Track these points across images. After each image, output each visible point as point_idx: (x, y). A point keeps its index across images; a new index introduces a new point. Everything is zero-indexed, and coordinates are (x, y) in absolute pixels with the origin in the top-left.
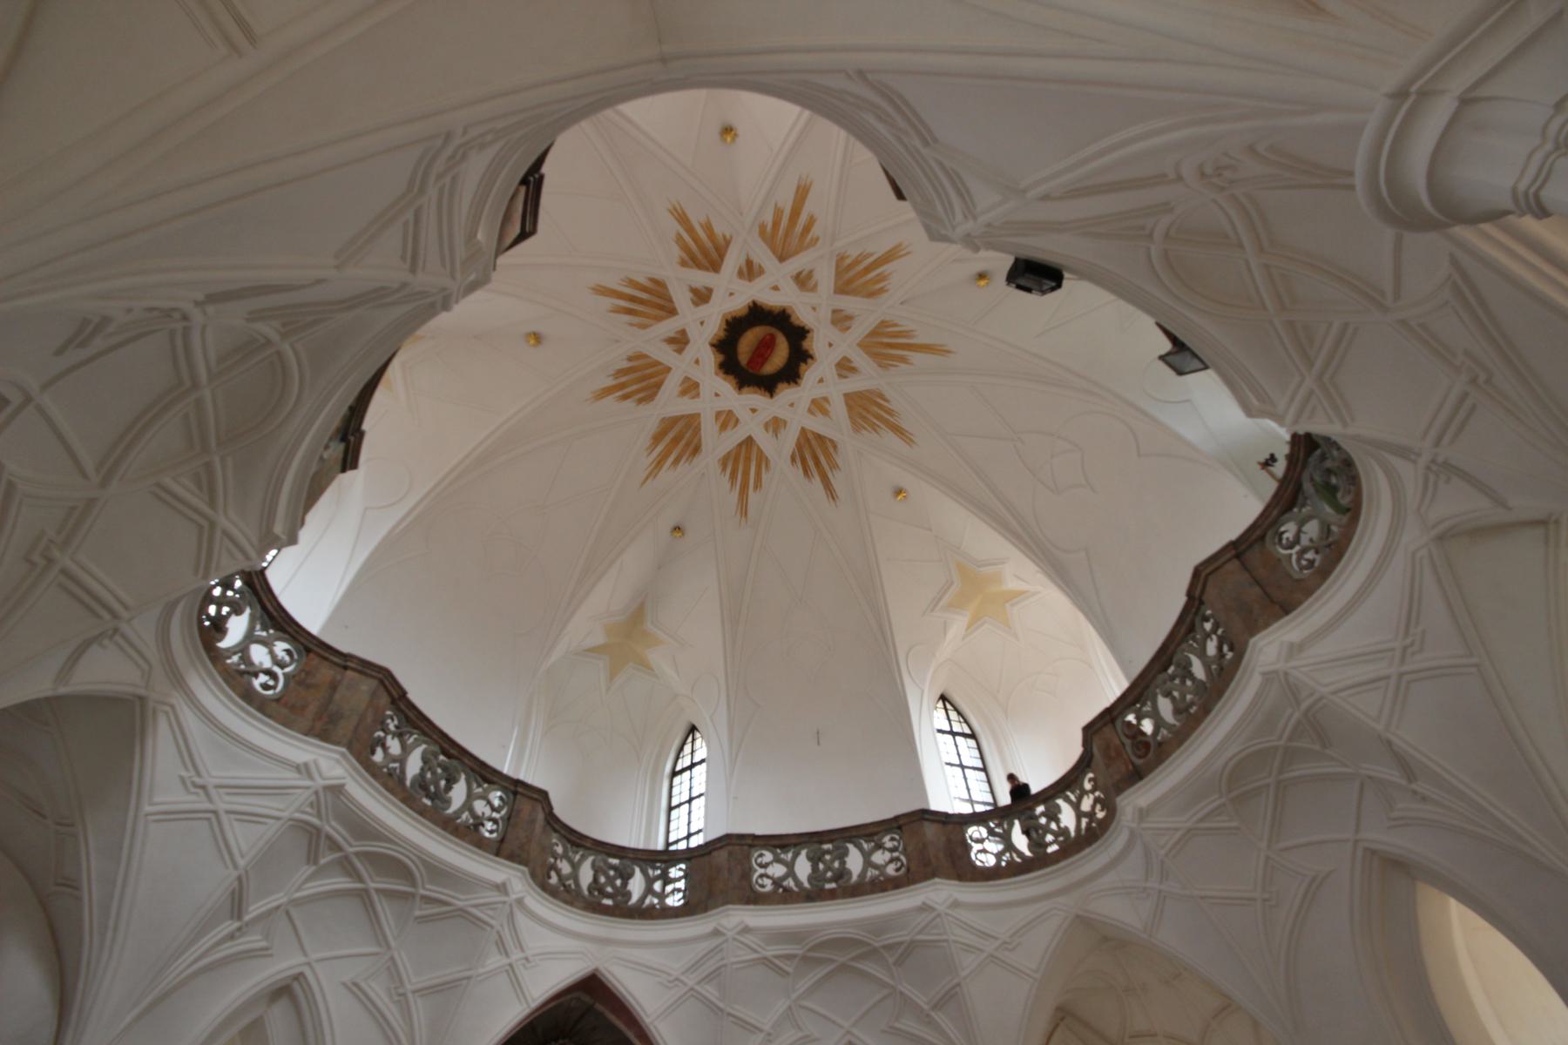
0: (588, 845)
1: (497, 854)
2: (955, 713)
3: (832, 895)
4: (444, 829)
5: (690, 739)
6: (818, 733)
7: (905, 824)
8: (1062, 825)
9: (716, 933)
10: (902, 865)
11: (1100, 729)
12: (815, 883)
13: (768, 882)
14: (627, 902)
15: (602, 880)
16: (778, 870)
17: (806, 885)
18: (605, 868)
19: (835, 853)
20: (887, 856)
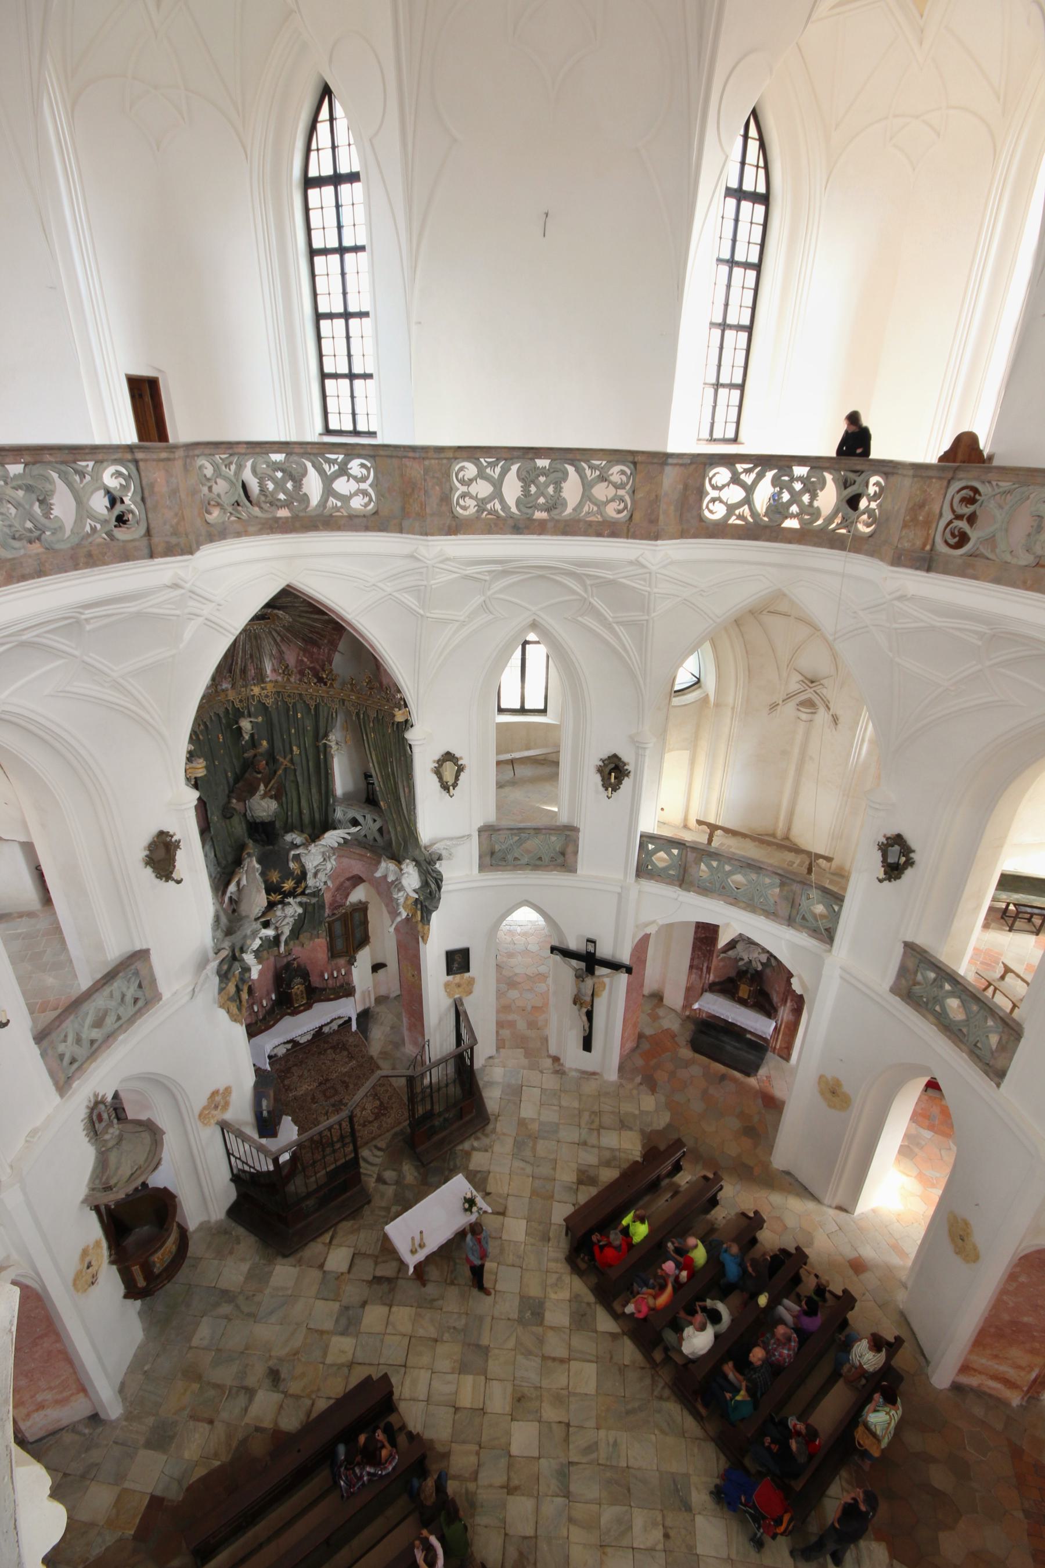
0: (243, 451)
1: (152, 556)
2: (757, 143)
3: (540, 528)
4: (76, 567)
5: (324, 113)
6: (547, 215)
7: (642, 463)
8: (816, 504)
9: (412, 557)
10: (626, 507)
11: (931, 478)
12: (525, 510)
13: (470, 502)
14: (307, 506)
15: (271, 486)
16: (482, 489)
17: (514, 509)
18: (270, 472)
19: (553, 476)
20: (611, 492)
